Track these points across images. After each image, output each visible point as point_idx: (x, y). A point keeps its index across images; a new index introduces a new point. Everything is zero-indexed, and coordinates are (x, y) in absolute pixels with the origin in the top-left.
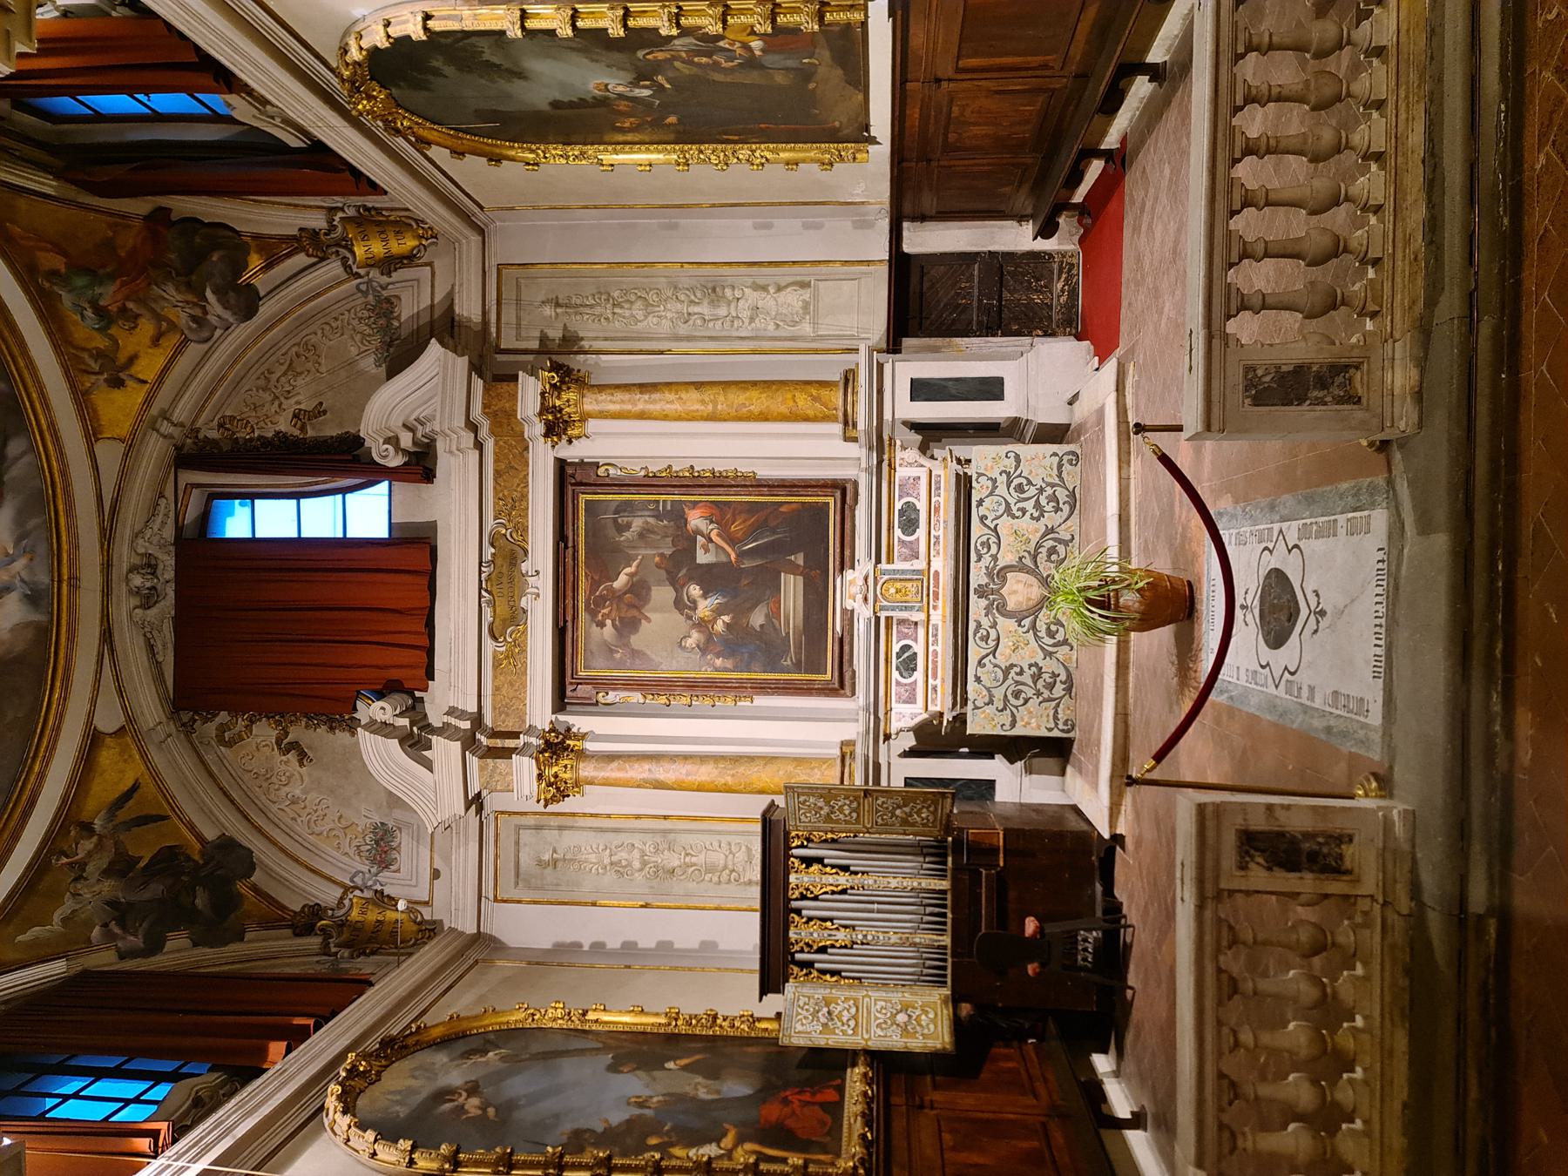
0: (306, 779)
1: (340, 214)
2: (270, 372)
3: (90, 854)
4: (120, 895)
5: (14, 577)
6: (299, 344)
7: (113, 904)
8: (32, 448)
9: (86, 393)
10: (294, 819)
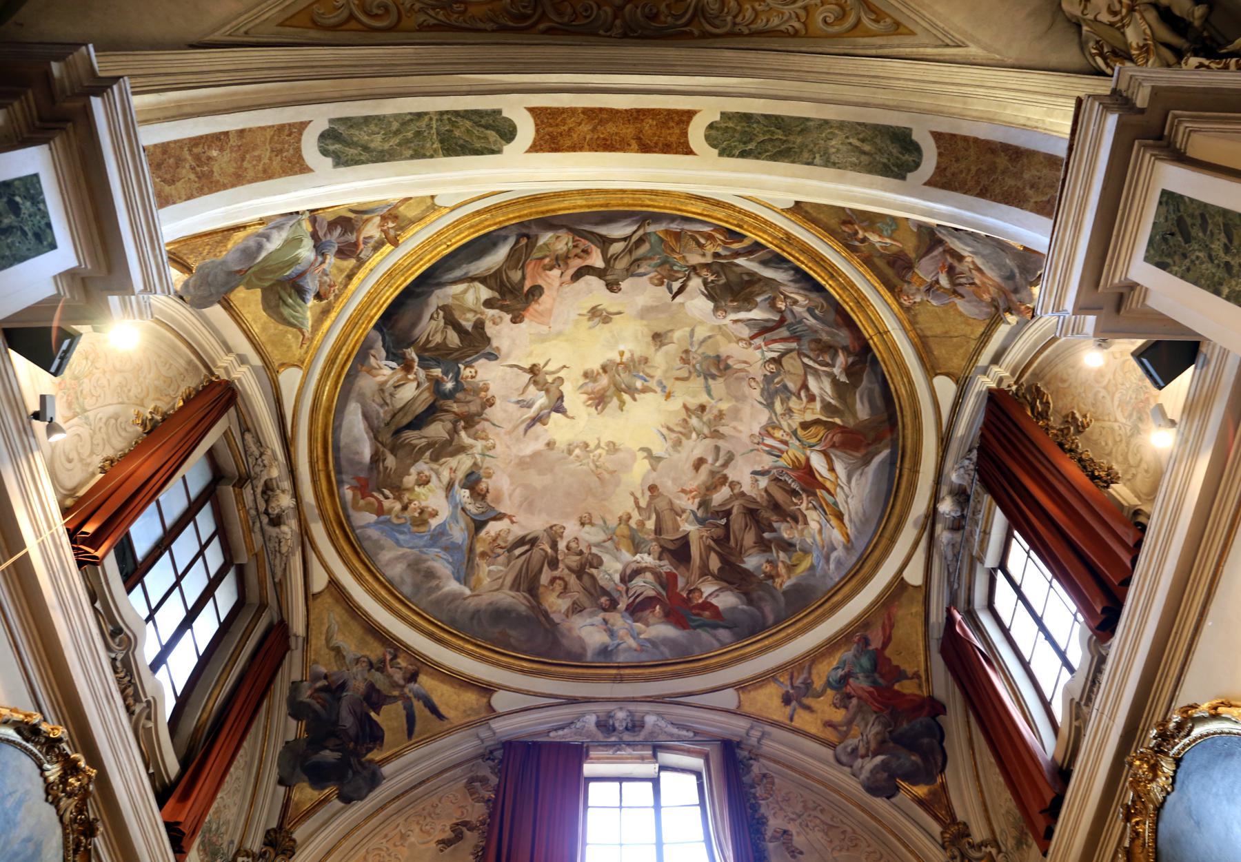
0: (423, 847)
1: (994, 851)
2: (822, 811)
3: (390, 676)
4: (349, 693)
5: (622, 639)
6: (854, 832)
7: (343, 686)
8: (723, 645)
9: (774, 679)
10: (386, 836)
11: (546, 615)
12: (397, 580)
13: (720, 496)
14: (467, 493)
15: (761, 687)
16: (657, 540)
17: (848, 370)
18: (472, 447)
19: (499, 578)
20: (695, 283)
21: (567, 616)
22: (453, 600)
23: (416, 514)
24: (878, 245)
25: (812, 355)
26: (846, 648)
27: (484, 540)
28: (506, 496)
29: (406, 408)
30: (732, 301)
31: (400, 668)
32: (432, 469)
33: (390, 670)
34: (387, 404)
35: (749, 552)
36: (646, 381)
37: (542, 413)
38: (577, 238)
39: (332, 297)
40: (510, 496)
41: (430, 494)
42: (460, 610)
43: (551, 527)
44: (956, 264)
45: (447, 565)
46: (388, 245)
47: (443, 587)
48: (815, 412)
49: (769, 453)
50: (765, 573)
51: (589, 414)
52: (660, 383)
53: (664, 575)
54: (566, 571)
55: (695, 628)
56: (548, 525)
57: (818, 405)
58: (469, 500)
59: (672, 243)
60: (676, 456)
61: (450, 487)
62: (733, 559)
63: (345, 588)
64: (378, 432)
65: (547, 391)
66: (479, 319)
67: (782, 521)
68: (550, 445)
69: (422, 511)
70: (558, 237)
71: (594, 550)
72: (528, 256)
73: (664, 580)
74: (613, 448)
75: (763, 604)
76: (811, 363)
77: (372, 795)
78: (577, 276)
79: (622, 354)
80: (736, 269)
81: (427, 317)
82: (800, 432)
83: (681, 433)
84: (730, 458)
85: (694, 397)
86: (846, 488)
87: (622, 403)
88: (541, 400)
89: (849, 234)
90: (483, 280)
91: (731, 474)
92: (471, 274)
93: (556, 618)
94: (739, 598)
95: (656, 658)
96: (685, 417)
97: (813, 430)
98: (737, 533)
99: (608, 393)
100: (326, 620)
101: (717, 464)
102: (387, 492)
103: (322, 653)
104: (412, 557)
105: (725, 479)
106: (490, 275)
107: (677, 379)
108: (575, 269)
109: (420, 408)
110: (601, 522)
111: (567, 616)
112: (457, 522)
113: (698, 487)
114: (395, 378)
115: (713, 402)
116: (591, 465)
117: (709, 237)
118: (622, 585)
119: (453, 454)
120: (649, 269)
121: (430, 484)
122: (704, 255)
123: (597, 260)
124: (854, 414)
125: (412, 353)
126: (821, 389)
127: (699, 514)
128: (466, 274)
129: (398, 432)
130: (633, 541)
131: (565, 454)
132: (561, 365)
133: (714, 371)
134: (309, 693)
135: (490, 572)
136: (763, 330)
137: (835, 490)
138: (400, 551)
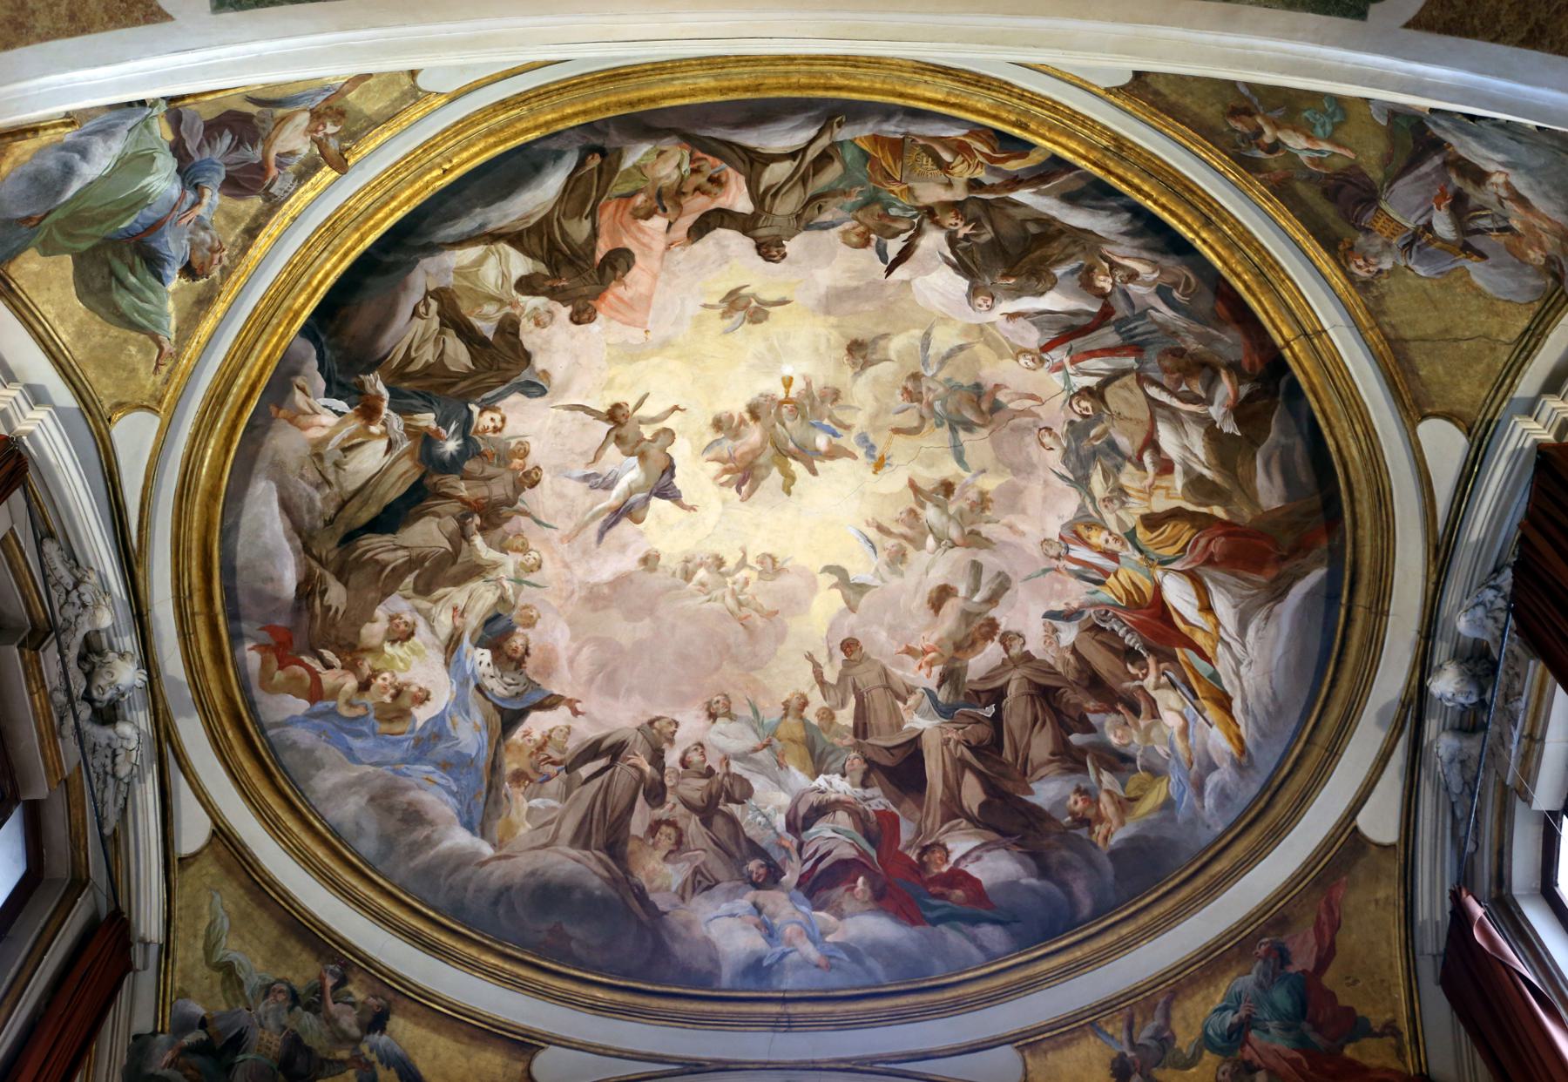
3: (331, 1020)
4: (249, 1056)
5: (790, 943)
7: (237, 1042)
8: (992, 957)
9: (1095, 1028)
11: (641, 895)
12: (347, 828)
13: (983, 661)
14: (486, 655)
15: (1068, 1043)
16: (857, 747)
17: (1240, 410)
18: (495, 565)
19: (551, 822)
20: (933, 241)
21: (683, 898)
22: (456, 868)
23: (387, 699)
24: (1303, 157)
25: (1165, 381)
26: (1240, 969)
27: (520, 748)
28: (563, 662)
29: (367, 492)
30: (1005, 276)
31: (353, 1004)
32: (418, 610)
33: (332, 1007)
34: (329, 483)
35: (1042, 772)
36: (835, 434)
37: (632, 499)
38: (700, 154)
39: (216, 273)
40: (571, 661)
41: (414, 658)
42: (471, 887)
43: (651, 723)
44: (1469, 189)
45: (446, 796)
46: (327, 168)
47: (440, 841)
48: (1172, 495)
49: (1081, 576)
50: (1072, 814)
51: (724, 502)
52: (863, 439)
53: (873, 817)
54: (681, 809)
55: (935, 922)
56: (646, 719)
57: (1178, 481)
58: (491, 671)
59: (887, 161)
60: (895, 581)
61: (452, 644)
62: (1009, 786)
63: (244, 846)
64: (312, 537)
65: (643, 457)
66: (507, 315)
67: (1106, 711)
68: (649, 561)
69: (399, 693)
70: (661, 153)
71: (736, 768)
72: (602, 191)
73: (874, 827)
74: (772, 566)
75: (1069, 876)
76: (1164, 397)
78: (700, 229)
79: (788, 382)
80: (1012, 211)
81: (405, 311)
82: (1142, 535)
83: (905, 537)
84: (1003, 585)
85: (930, 466)
86: (1236, 646)
87: (790, 478)
88: (631, 473)
89: (1244, 135)
90: (515, 239)
91: (1005, 618)
92: (490, 228)
93: (661, 901)
94: (1021, 862)
95: (858, 982)
96: (914, 506)
97: (1168, 529)
98: (1017, 735)
99: (762, 460)
100: (205, 910)
101: (977, 598)
102: (328, 655)
103: (197, 975)
104: (379, 782)
105: (992, 625)
106: (529, 230)
107: (897, 431)
108: (696, 216)
109: (393, 491)
110: (749, 713)
111: (683, 898)
112: (468, 713)
113: (940, 642)
114: (345, 432)
115: (967, 475)
116: (730, 601)
117: (960, 148)
118: (790, 837)
119: (458, 581)
120: (841, 214)
121: (415, 639)
122: (950, 185)
123: (738, 199)
124: (1252, 499)
125: (376, 384)
126: (1185, 447)
127: (942, 696)
128: (481, 226)
129: (350, 537)
130: (812, 752)
131: (679, 580)
132: (670, 405)
133: (969, 415)
134: (168, 1056)
135: (531, 809)
136: (1068, 332)
137: (1214, 650)
138: (355, 772)
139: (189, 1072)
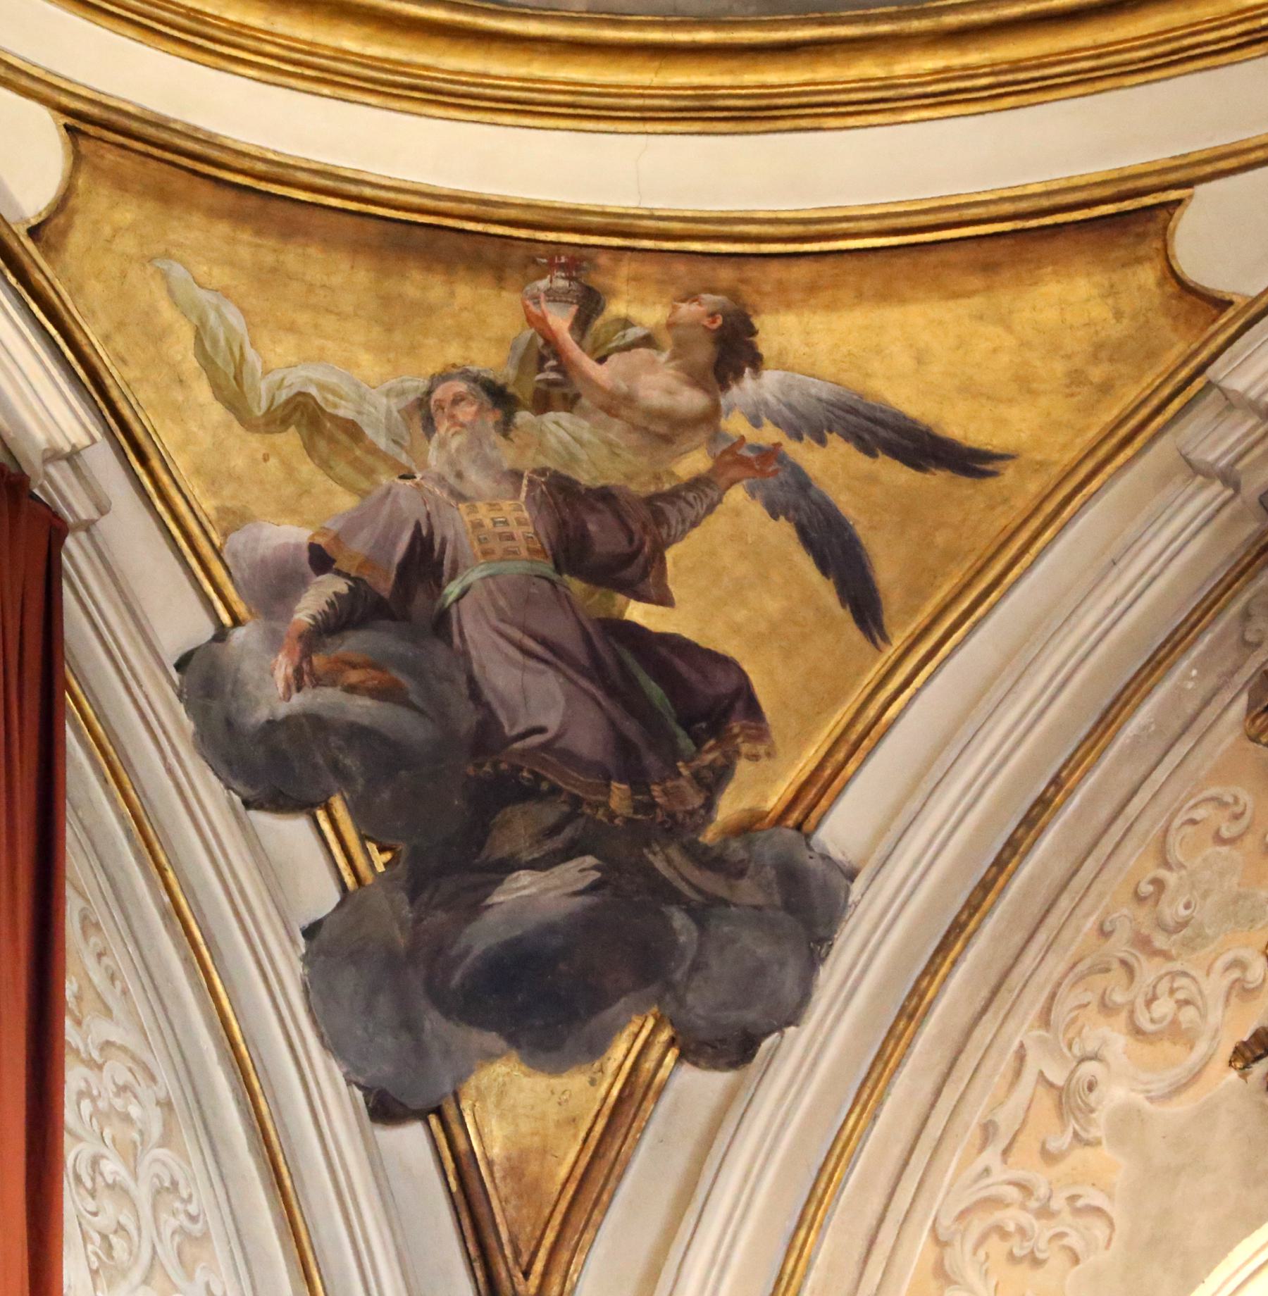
0: (1182, 1107)
4: (473, 576)
10: (988, 1131)
31: (648, 341)
33: (600, 373)
63: (161, 124)
77: (829, 978)
100: (167, 313)
103: (239, 462)
134: (283, 667)
139: (354, 676)
